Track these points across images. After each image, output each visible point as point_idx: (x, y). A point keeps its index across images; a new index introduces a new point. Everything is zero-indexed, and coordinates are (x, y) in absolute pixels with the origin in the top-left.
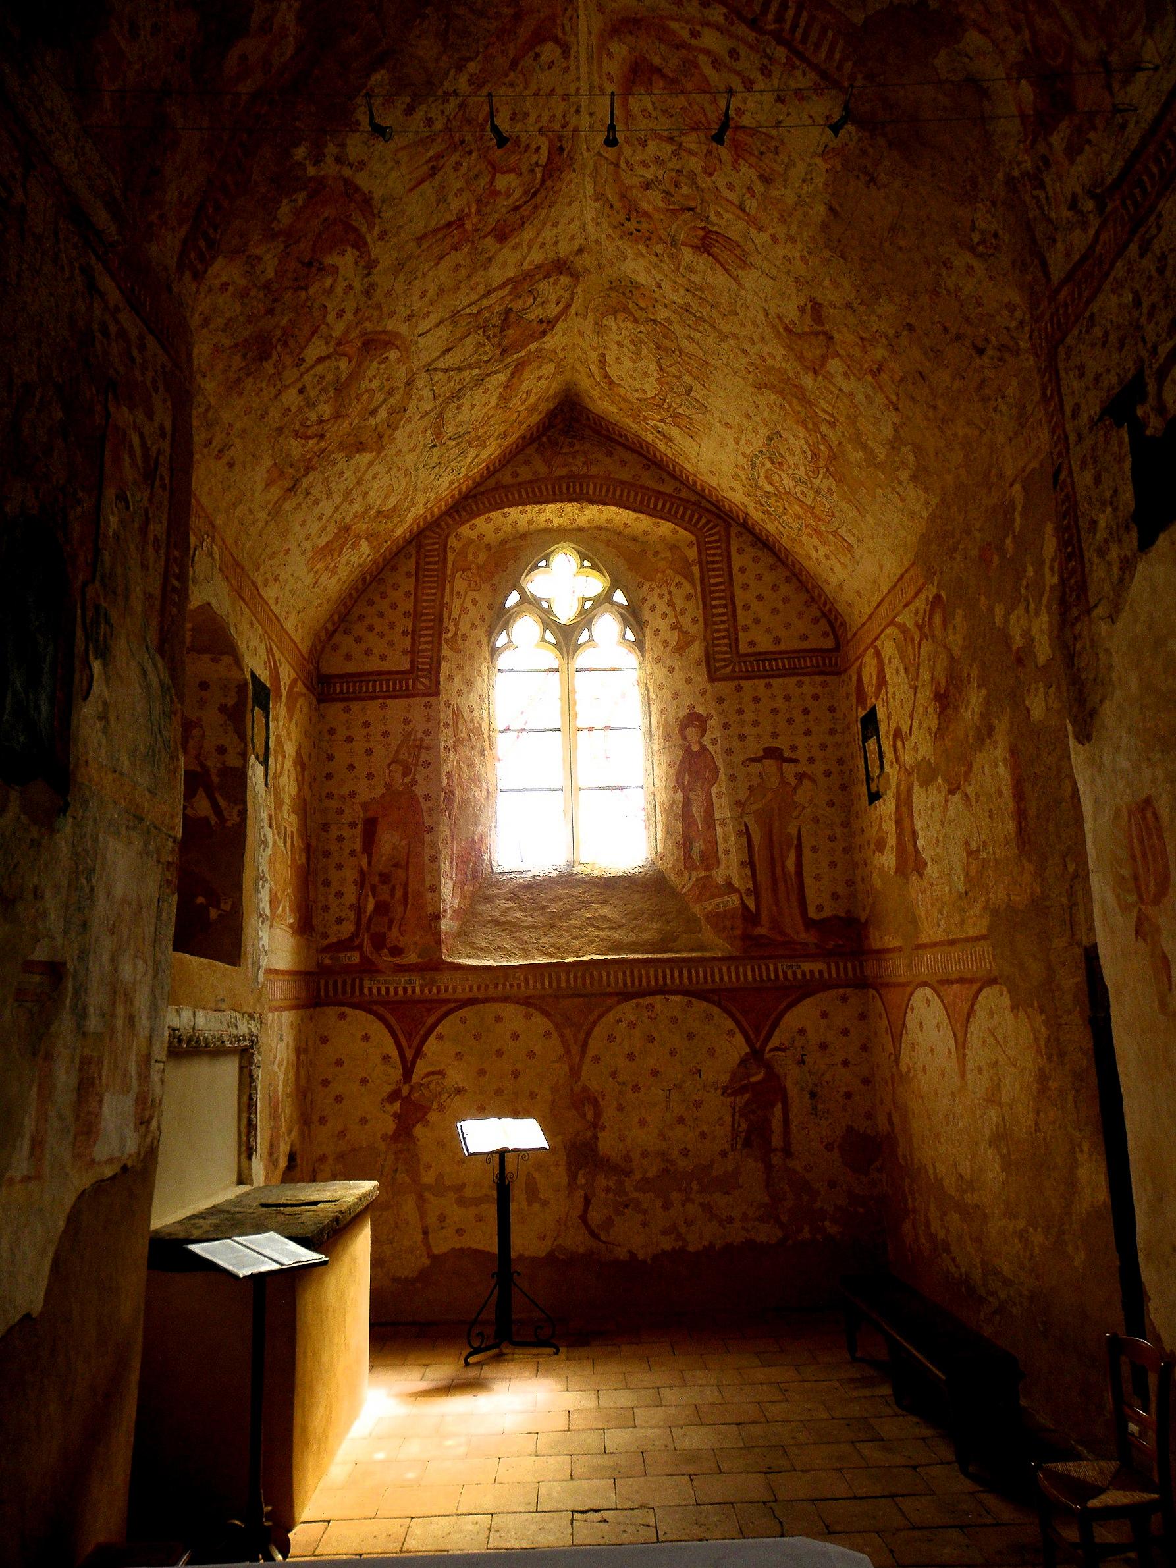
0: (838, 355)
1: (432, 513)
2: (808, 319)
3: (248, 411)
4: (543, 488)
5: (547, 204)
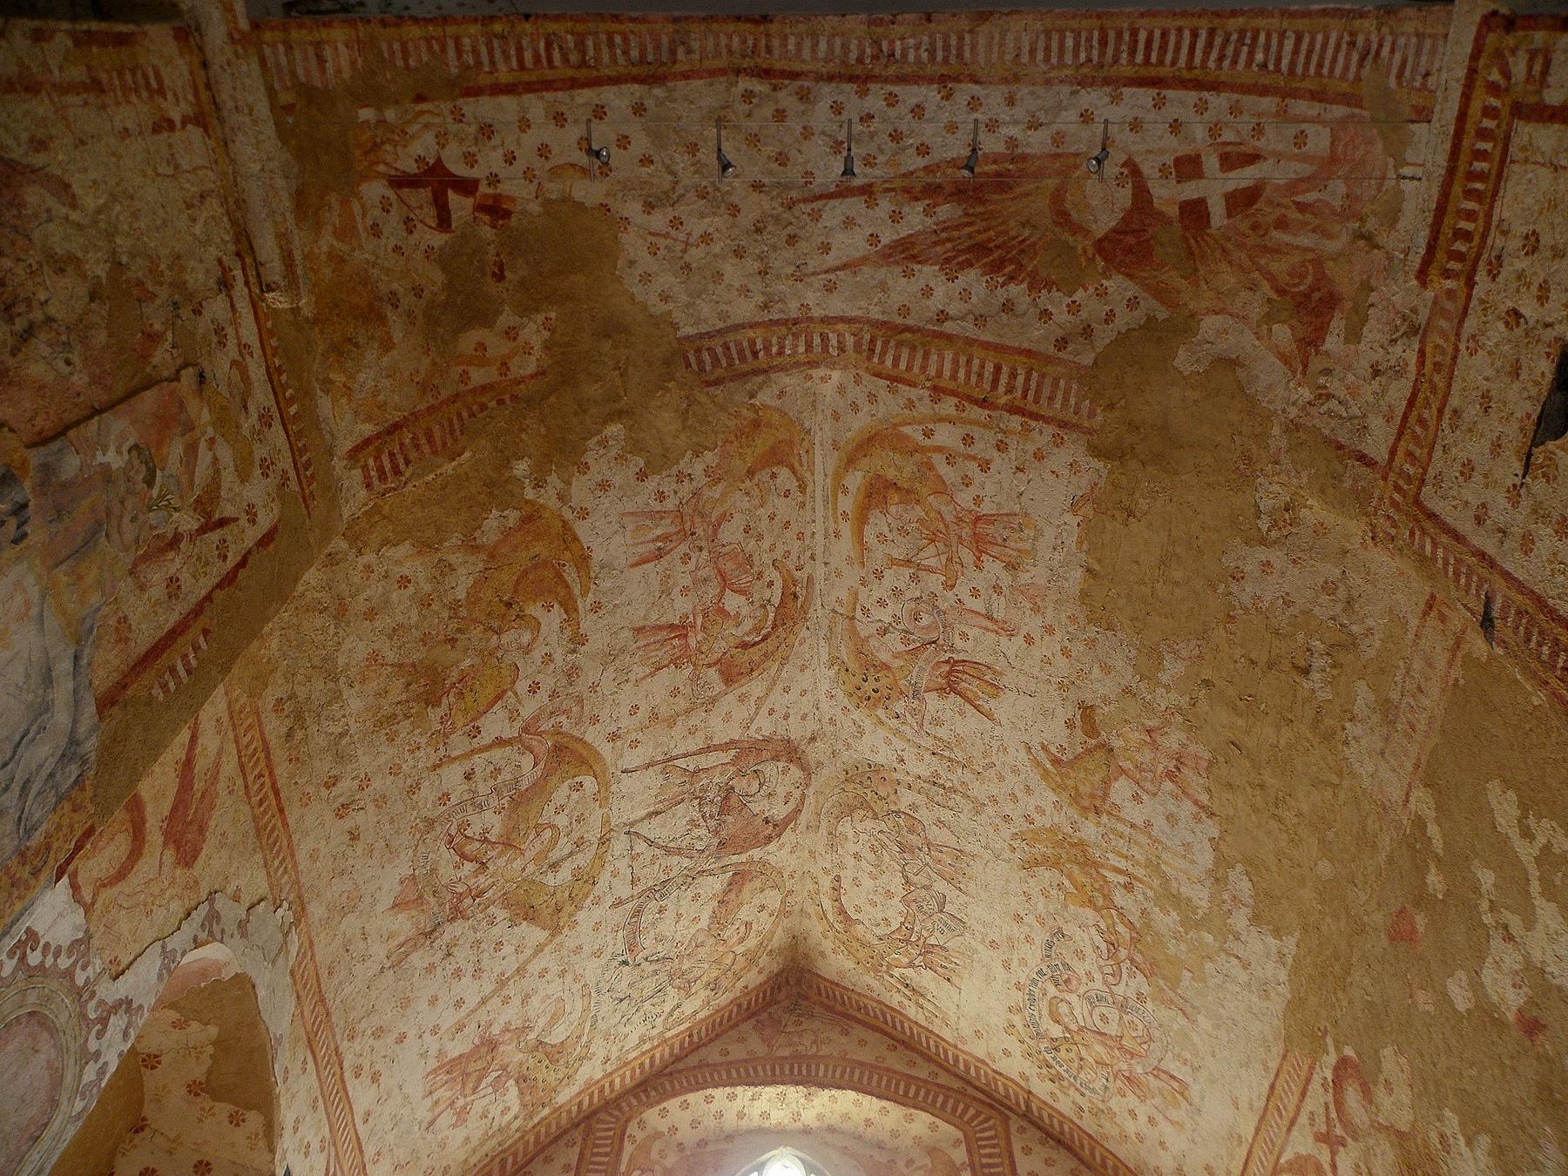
0: (1123, 771)
1: (612, 1084)
2: (1079, 732)
3: (394, 771)
4: (760, 1069)
5: (778, 655)
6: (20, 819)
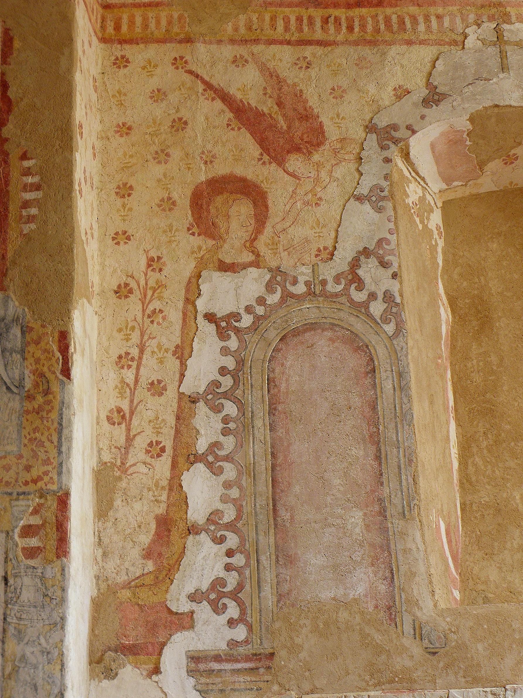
6: (8, 388)
